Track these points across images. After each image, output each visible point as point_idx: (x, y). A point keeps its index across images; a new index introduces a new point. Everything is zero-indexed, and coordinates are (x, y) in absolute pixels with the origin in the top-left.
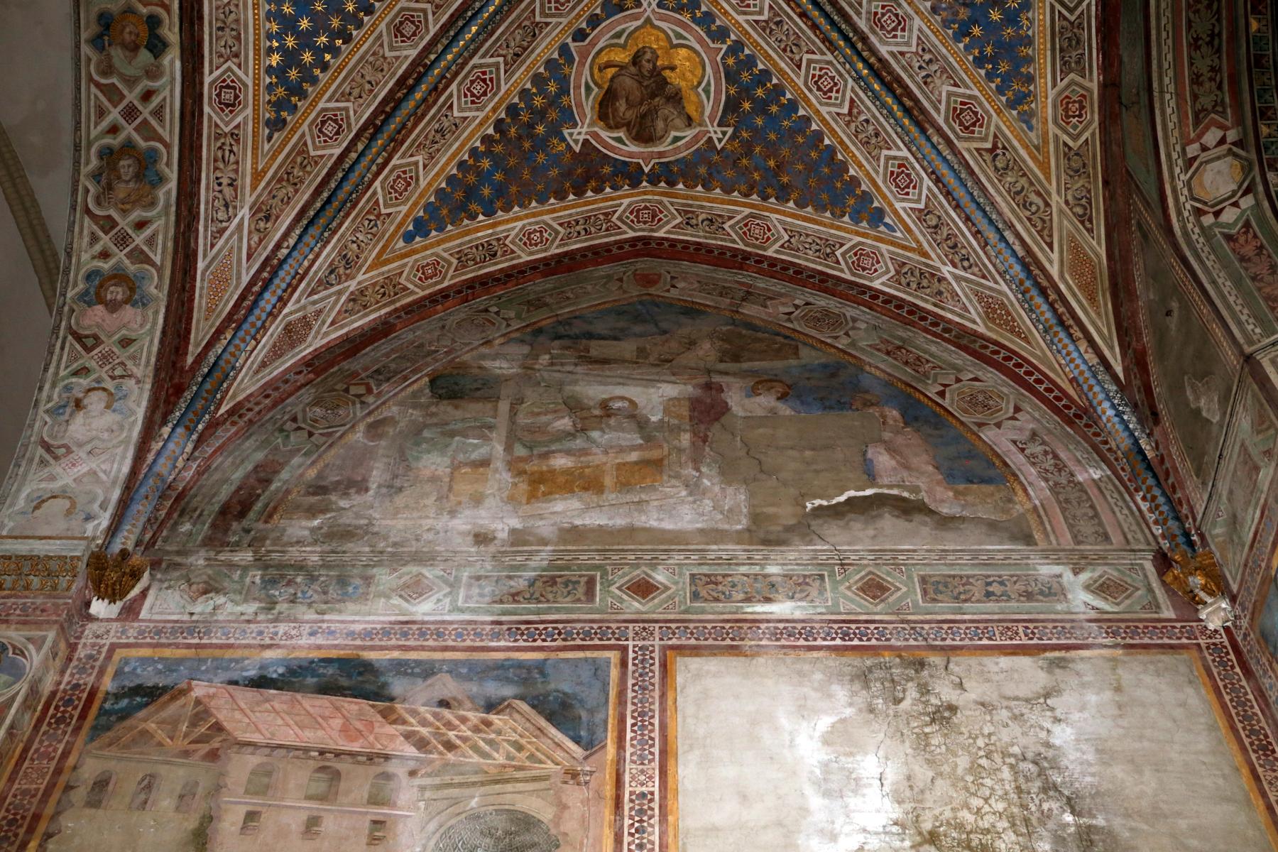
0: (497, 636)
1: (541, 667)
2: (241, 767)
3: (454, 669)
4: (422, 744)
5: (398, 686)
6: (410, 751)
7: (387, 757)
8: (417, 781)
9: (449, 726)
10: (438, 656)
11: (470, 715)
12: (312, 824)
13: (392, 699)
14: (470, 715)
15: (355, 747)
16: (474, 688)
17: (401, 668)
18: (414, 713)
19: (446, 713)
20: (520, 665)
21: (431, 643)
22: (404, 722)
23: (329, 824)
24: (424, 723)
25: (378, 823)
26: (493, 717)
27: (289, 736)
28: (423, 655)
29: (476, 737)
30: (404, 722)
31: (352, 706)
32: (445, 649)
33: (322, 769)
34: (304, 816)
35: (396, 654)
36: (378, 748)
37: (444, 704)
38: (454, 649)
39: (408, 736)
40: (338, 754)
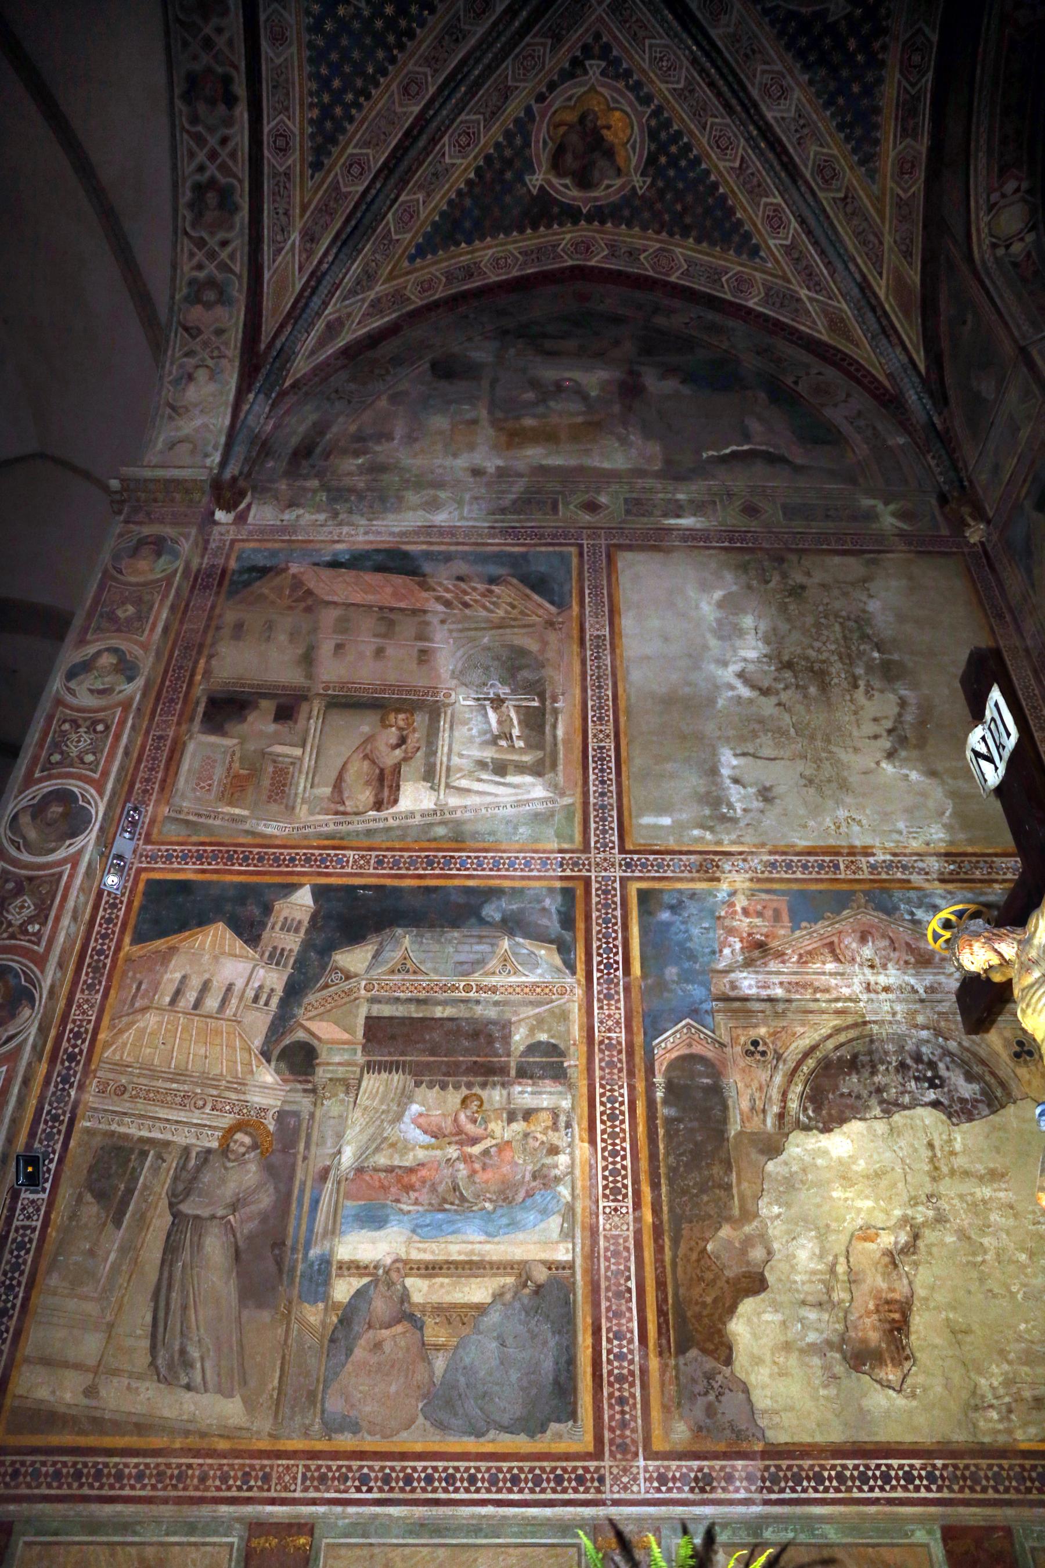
0: (494, 536)
1: (524, 556)
2: (329, 617)
3: (464, 556)
4: (447, 604)
5: (427, 567)
6: (440, 608)
7: (425, 612)
8: (446, 627)
9: (465, 593)
10: (453, 548)
11: (479, 586)
12: (379, 652)
13: (424, 575)
14: (479, 586)
15: (402, 605)
16: (479, 569)
17: (428, 556)
18: (440, 584)
19: (463, 585)
20: (510, 555)
21: (447, 540)
22: (434, 590)
23: (390, 651)
24: (447, 590)
25: (423, 652)
26: (493, 587)
27: (358, 598)
28: (443, 548)
29: (484, 600)
30: (434, 590)
31: (398, 580)
32: (458, 544)
33: (383, 618)
34: (373, 647)
35: (424, 547)
36: (418, 606)
37: (460, 579)
38: (463, 544)
39: (438, 599)
40: (392, 609)
